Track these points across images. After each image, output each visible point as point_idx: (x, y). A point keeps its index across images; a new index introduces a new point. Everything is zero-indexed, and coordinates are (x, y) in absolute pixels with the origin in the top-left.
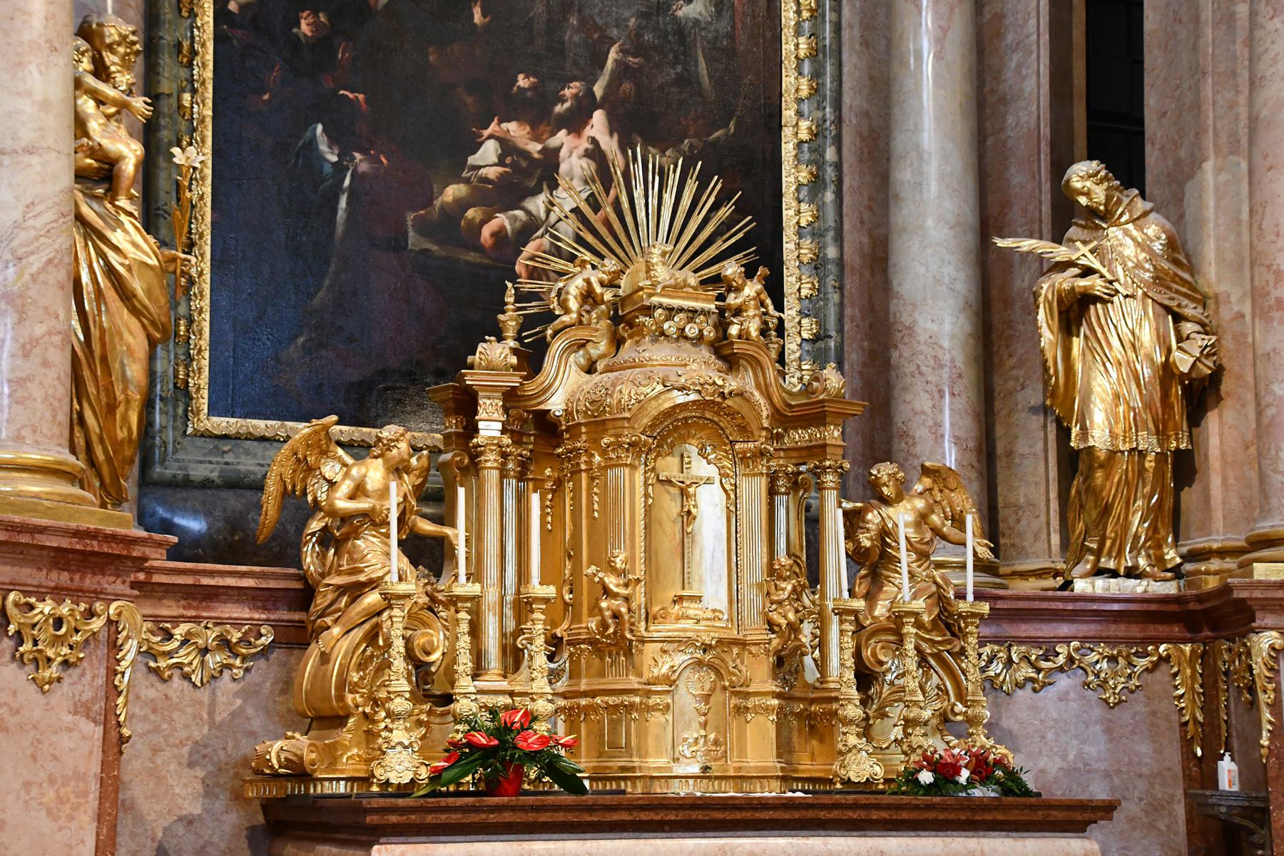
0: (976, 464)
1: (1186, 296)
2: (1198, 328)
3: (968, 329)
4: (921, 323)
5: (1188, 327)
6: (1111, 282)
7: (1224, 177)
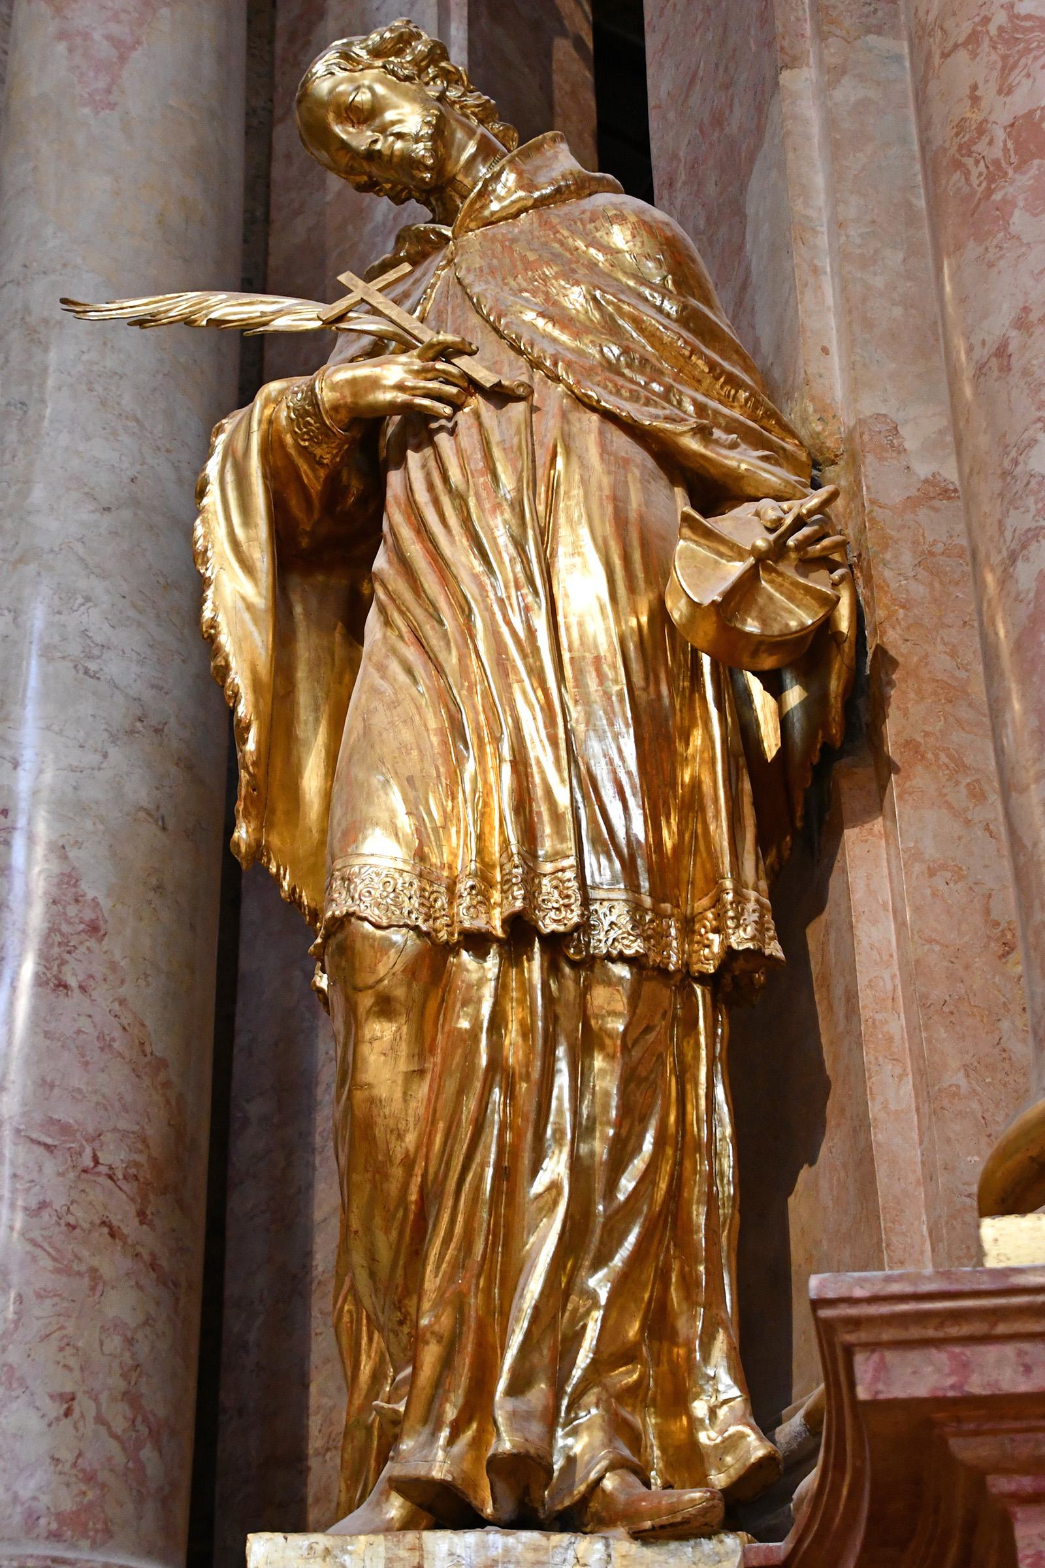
0: (130, 1227)
3: (139, 790)
7: (848, 92)
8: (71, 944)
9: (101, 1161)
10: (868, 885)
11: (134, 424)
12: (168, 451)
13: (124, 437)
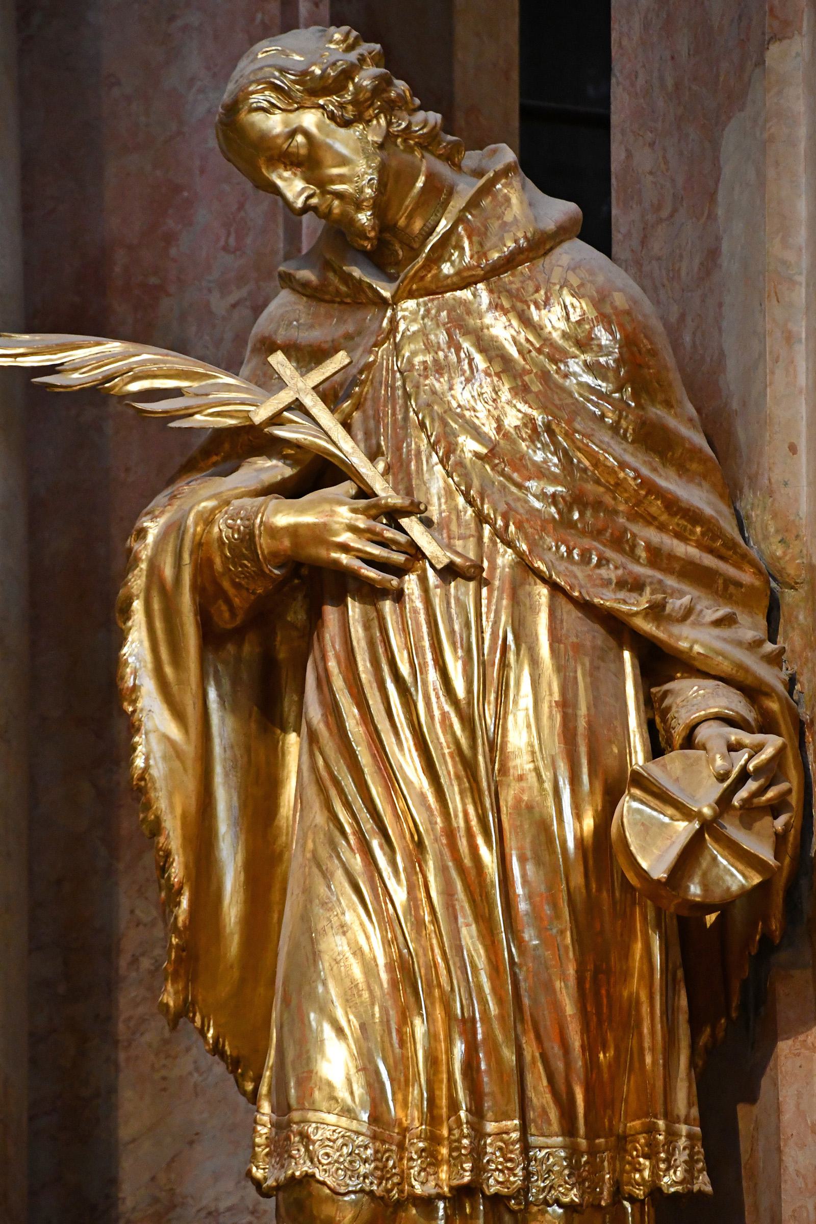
1: (692, 573)
2: (729, 701)
5: (693, 699)
6: (393, 516)
10: (798, 1105)
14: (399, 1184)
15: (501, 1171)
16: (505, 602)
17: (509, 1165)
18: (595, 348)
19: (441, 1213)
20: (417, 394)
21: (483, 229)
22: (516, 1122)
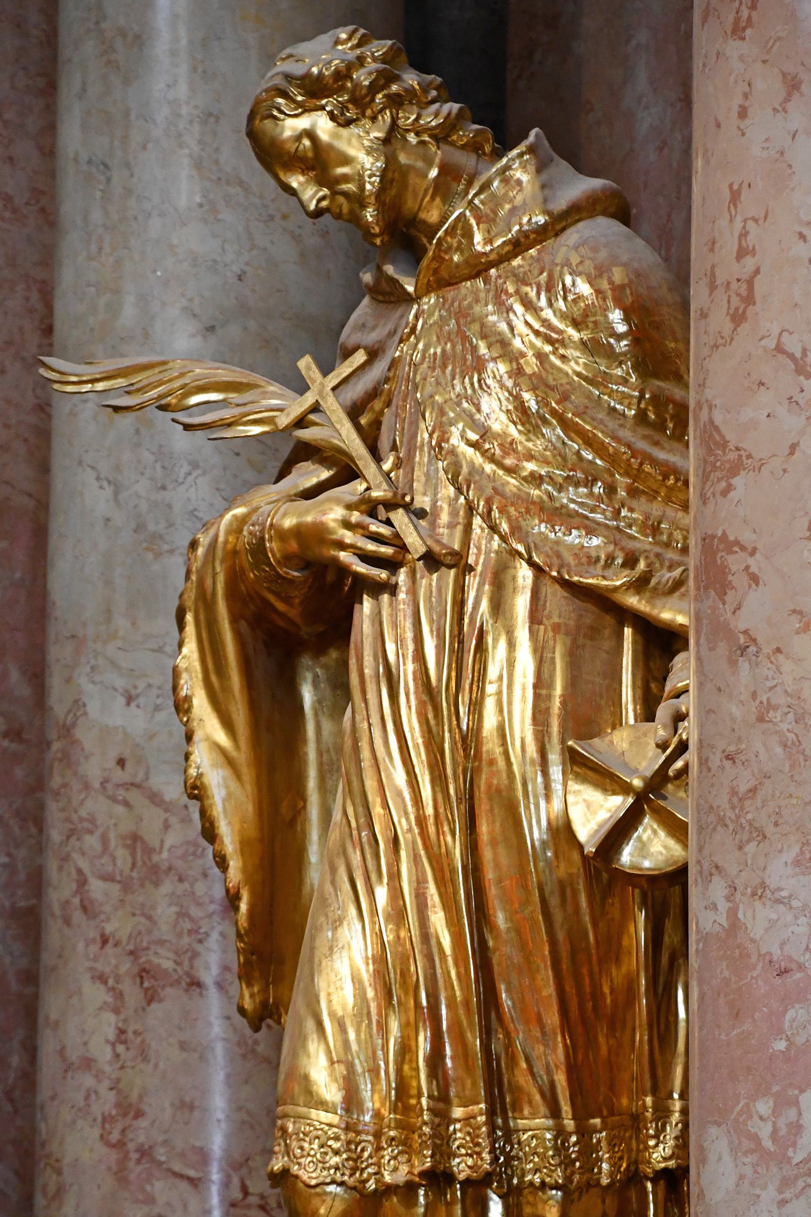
4: (93, 709)
8: (202, 931)
9: (251, 1190)
11: (238, 189)
12: (285, 217)
13: (226, 215)
14: (375, 1174)
15: (471, 1156)
16: (487, 587)
17: (477, 1149)
18: (591, 325)
19: (422, 1199)
20: (424, 386)
21: (492, 215)
22: (483, 1106)
